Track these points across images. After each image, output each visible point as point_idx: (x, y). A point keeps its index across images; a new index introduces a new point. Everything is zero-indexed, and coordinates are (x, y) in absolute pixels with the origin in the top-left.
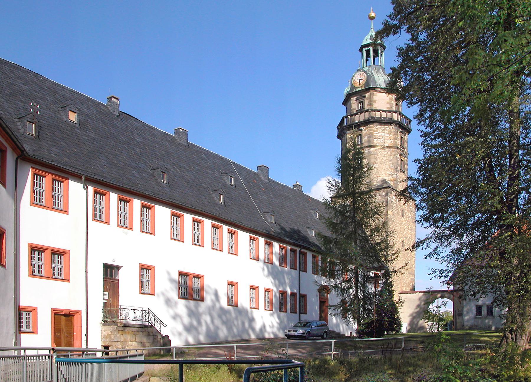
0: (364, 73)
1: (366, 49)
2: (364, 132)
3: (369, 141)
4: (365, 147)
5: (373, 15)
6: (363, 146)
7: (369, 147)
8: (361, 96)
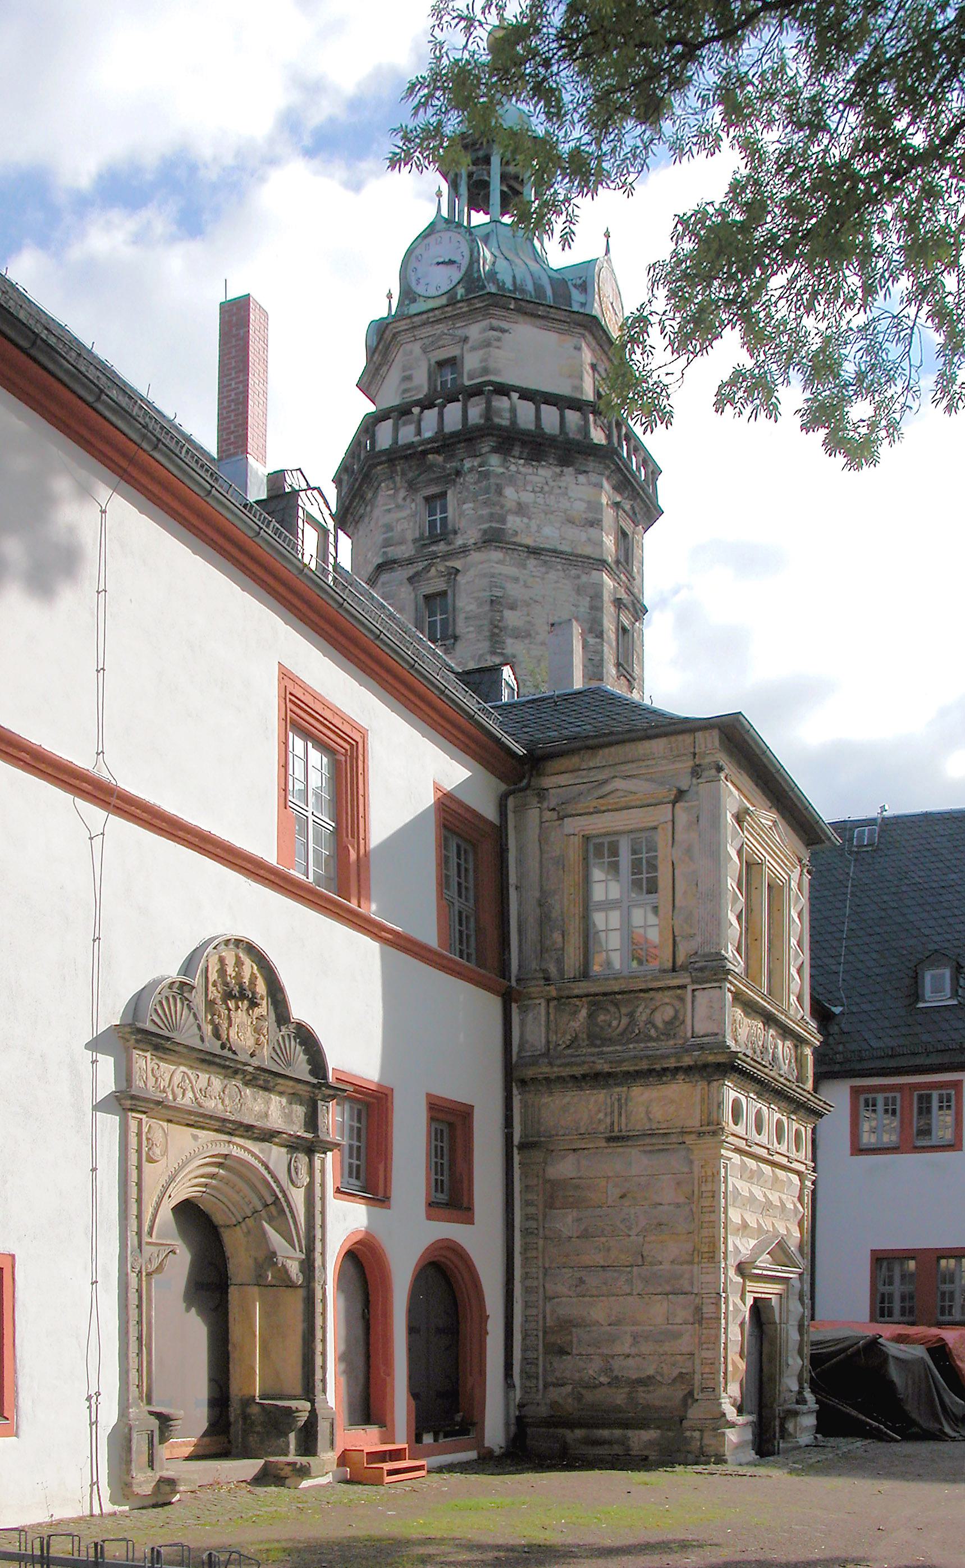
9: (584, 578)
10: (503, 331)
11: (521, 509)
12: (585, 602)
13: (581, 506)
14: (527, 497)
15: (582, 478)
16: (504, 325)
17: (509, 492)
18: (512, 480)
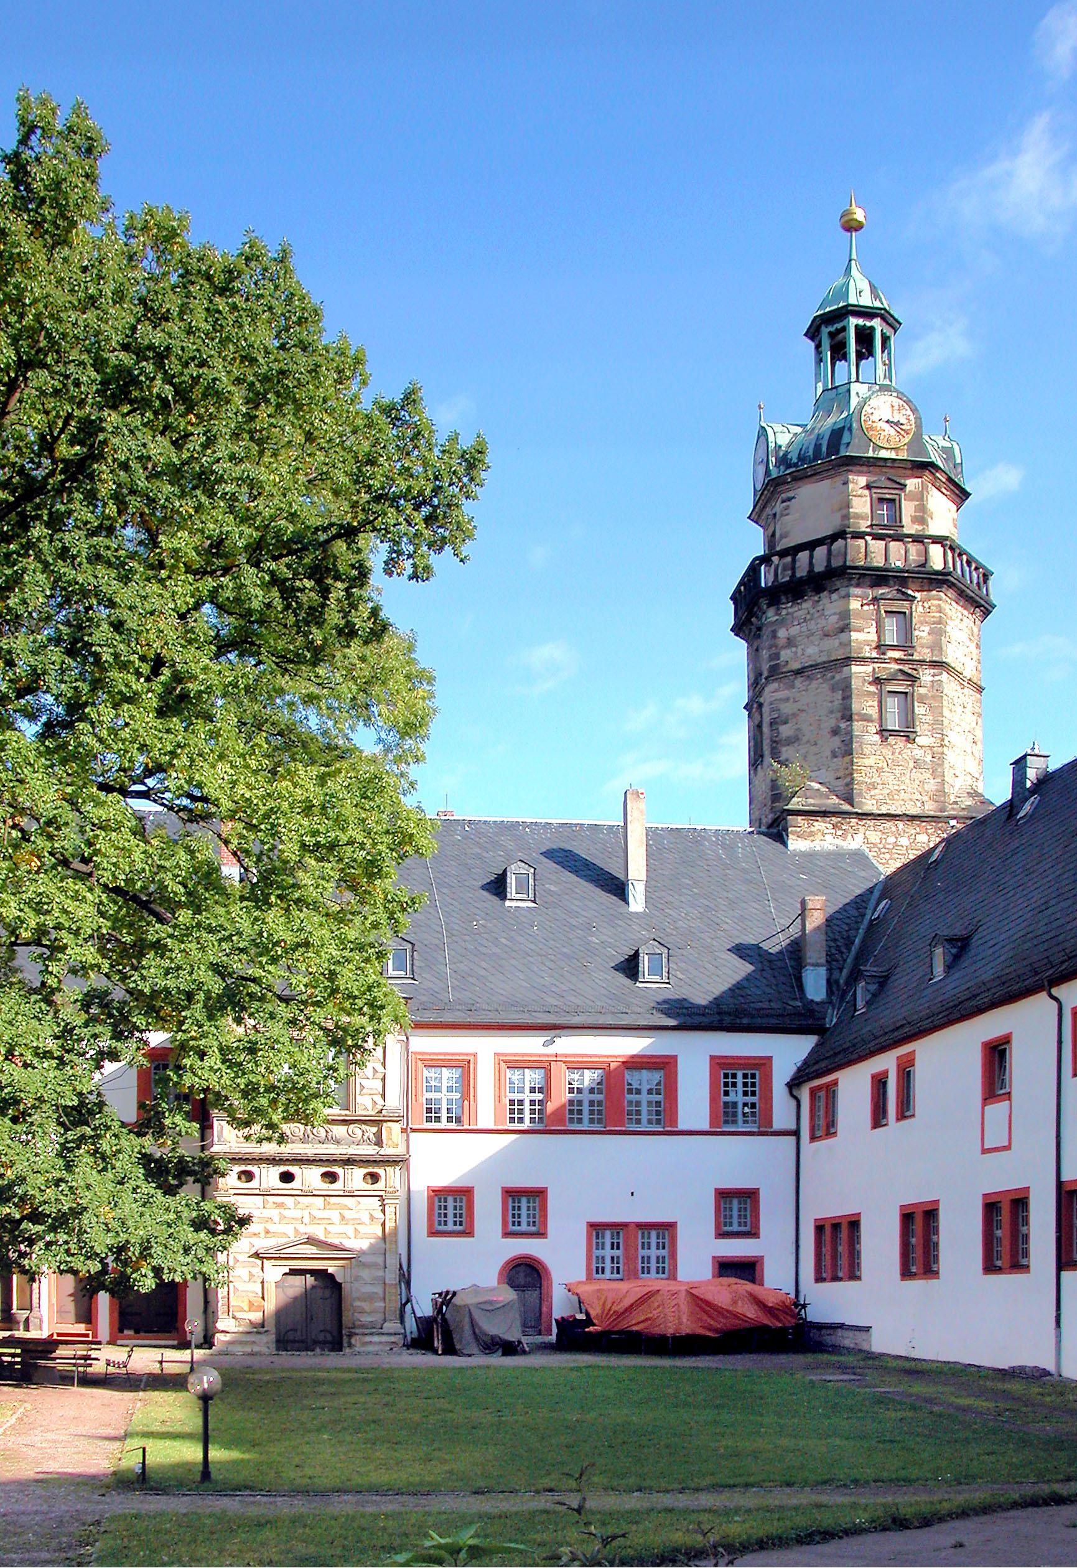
0: (907, 407)
1: (861, 322)
2: (918, 609)
3: (937, 646)
4: (922, 662)
5: (859, 215)
6: (915, 657)
7: (939, 665)
8: (889, 479)
9: (838, 677)
10: (789, 499)
11: (790, 642)
12: (839, 695)
13: (835, 618)
14: (794, 631)
15: (835, 596)
16: (790, 494)
17: (782, 633)
18: (782, 623)
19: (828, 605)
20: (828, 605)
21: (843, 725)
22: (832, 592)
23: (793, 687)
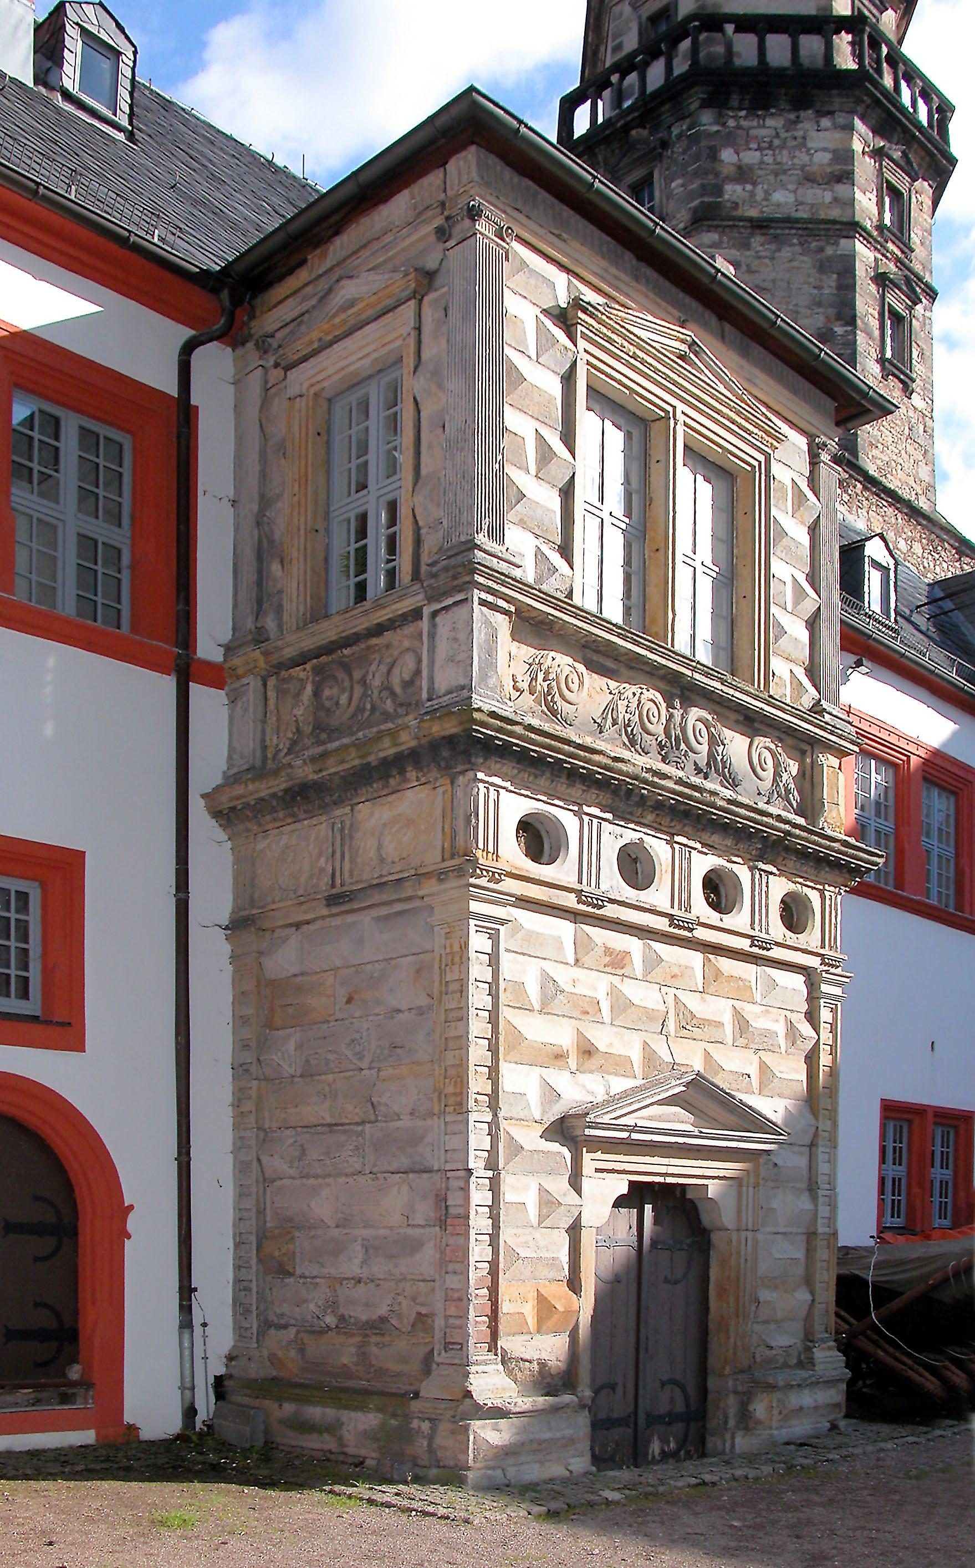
9: (829, 251)
11: (743, 174)
12: (831, 281)
13: (825, 158)
14: (751, 157)
15: (825, 122)
17: (727, 155)
18: (729, 139)
19: (813, 134)
20: (813, 134)
21: (839, 330)
22: (821, 114)
23: (747, 246)
